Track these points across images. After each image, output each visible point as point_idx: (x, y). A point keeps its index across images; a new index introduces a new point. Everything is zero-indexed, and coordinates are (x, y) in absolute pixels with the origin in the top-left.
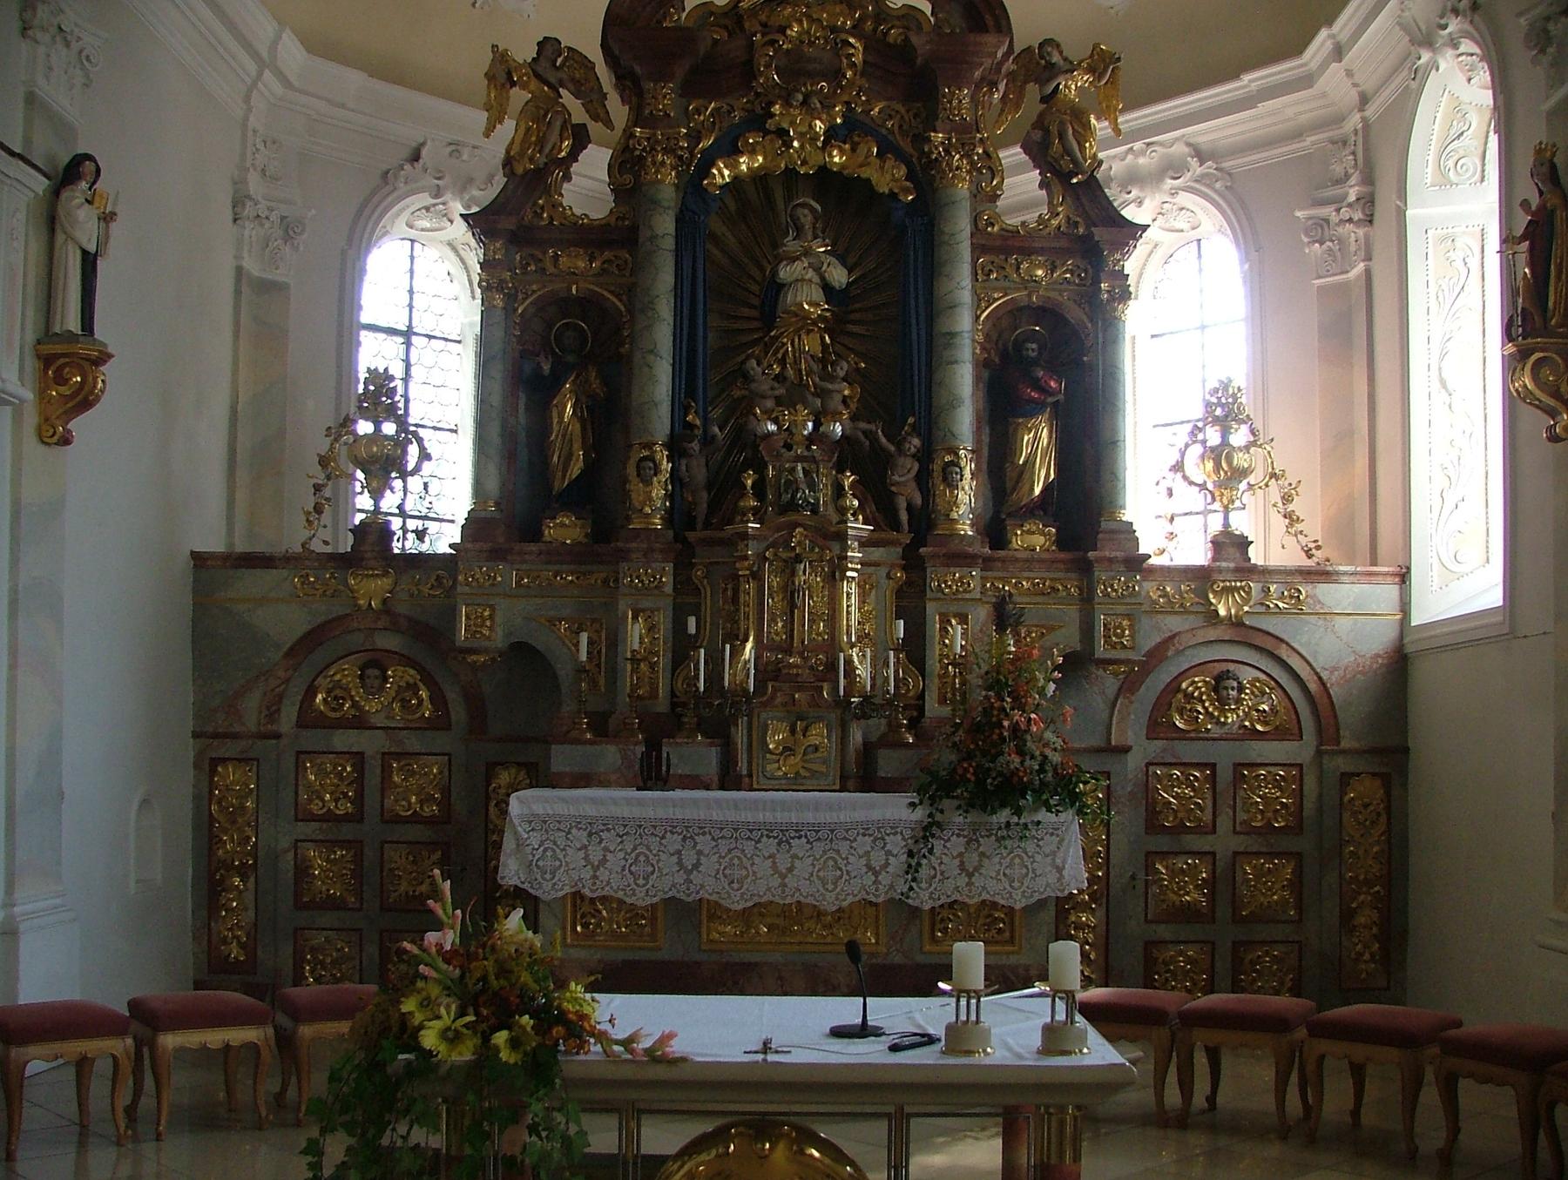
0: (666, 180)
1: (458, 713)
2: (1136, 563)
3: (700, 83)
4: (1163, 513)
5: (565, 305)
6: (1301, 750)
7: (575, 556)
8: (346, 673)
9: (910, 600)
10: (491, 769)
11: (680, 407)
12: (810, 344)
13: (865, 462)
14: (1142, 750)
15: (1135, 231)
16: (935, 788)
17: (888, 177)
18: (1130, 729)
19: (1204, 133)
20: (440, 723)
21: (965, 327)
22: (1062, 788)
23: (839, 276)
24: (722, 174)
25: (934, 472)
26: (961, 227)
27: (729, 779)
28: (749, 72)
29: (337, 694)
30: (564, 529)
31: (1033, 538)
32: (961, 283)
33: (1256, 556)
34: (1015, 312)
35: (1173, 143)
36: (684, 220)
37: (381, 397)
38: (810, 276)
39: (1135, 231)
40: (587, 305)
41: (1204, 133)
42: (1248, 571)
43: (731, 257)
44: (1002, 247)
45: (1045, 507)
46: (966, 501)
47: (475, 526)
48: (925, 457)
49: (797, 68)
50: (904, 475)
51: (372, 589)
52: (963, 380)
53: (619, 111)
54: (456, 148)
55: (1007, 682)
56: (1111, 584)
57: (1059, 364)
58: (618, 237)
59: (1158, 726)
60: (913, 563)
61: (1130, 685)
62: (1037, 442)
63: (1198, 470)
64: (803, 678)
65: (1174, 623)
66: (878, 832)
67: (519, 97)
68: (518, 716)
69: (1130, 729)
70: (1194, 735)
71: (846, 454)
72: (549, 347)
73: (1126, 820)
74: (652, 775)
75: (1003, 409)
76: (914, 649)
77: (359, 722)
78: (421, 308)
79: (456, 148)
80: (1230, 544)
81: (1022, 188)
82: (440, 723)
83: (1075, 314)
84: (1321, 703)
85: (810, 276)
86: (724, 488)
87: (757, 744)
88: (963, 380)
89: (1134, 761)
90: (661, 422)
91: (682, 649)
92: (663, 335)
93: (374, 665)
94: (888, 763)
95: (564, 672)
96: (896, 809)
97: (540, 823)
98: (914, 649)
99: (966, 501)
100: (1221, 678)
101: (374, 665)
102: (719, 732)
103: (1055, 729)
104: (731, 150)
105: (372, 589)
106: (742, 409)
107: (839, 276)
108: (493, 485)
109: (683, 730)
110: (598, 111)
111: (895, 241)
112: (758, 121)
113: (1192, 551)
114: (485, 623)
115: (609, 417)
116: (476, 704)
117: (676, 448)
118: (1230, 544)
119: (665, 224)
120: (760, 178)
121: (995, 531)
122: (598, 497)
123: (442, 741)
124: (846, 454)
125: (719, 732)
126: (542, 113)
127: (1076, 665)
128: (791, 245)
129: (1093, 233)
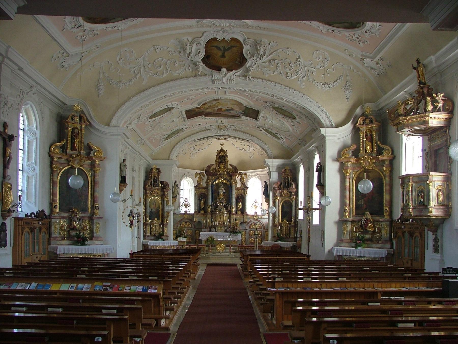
0: (210, 184)
1: (193, 226)
2: (247, 215)
3: (213, 175)
4: (250, 210)
5: (202, 193)
6: (262, 230)
7: (204, 214)
8: (184, 223)
9: (229, 218)
10: (196, 231)
11: (211, 203)
12: (221, 197)
13: (226, 207)
14: (249, 229)
15: (248, 188)
16: (231, 232)
17: (228, 183)
18: (248, 228)
19: (258, 173)
20: (192, 227)
21: (234, 196)
22: (240, 232)
23: (224, 191)
24: (215, 183)
25: (231, 208)
26: (234, 188)
27: (216, 232)
28: (217, 174)
29: (183, 225)
30: (202, 212)
31: (239, 213)
32: (234, 193)
33: (258, 214)
34: (238, 194)
35: (256, 173)
36: (212, 187)
37: (186, 200)
38: (222, 191)
39: (248, 188)
40: (204, 194)
41: (258, 173)
42: (257, 215)
43: (216, 194)
44: (237, 189)
45: (241, 210)
46: (234, 210)
47: (195, 212)
48: (231, 206)
49: (221, 174)
50: (229, 208)
51: (186, 216)
52: (234, 201)
53: (206, 177)
54: (188, 173)
55: (236, 224)
56: (245, 217)
57: (242, 198)
58: (207, 188)
59: (250, 227)
60: (230, 215)
61: (247, 224)
62: (240, 205)
63: (253, 206)
64: (221, 224)
65: (251, 219)
66: (227, 235)
67: (198, 176)
68: (199, 227)
69: (248, 228)
70: (253, 228)
71: (225, 207)
72: (201, 196)
73: (247, 235)
74: (210, 231)
75: (237, 202)
76: (230, 222)
77: (185, 227)
78: (187, 191)
79: (188, 173)
80: (256, 213)
81: (239, 185)
82: (192, 227)
83: (243, 194)
84: (263, 226)
85: (222, 191)
86: (215, 209)
87: (218, 229)
88: (234, 201)
89: (248, 230)
90: (210, 204)
91: (212, 222)
92: (210, 197)
93: (186, 222)
94: (227, 230)
95: (202, 223)
96: (228, 234)
97: (202, 235)
98: (230, 222)
99: (234, 210)
100: (255, 224)
101: (186, 222)
102: (215, 228)
103: (239, 227)
104: (215, 181)
105: (186, 216)
106: (216, 203)
107: (224, 191)
108: (197, 208)
109: (212, 228)
110: (204, 176)
111: (228, 188)
112: (218, 179)
113: (253, 213)
114: (196, 219)
115: (206, 203)
116: (194, 226)
117: (211, 206)
118: (256, 213)
119: (210, 188)
120: (218, 183)
121: (236, 212)
122: (205, 209)
123: (192, 229)
124: (225, 207)
125: (215, 228)
126: (200, 178)
127: (242, 223)
128: (220, 188)
129: (245, 188)
